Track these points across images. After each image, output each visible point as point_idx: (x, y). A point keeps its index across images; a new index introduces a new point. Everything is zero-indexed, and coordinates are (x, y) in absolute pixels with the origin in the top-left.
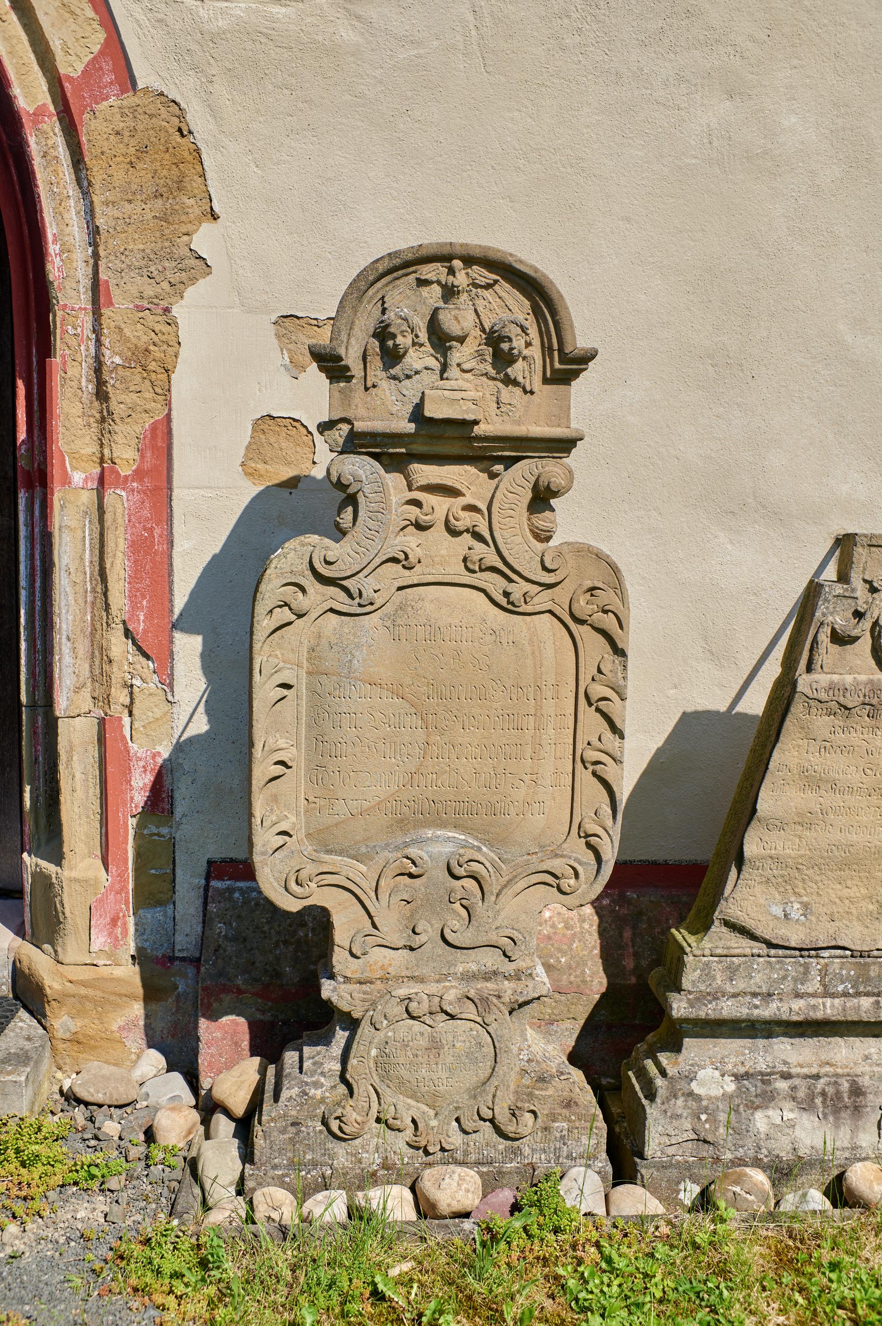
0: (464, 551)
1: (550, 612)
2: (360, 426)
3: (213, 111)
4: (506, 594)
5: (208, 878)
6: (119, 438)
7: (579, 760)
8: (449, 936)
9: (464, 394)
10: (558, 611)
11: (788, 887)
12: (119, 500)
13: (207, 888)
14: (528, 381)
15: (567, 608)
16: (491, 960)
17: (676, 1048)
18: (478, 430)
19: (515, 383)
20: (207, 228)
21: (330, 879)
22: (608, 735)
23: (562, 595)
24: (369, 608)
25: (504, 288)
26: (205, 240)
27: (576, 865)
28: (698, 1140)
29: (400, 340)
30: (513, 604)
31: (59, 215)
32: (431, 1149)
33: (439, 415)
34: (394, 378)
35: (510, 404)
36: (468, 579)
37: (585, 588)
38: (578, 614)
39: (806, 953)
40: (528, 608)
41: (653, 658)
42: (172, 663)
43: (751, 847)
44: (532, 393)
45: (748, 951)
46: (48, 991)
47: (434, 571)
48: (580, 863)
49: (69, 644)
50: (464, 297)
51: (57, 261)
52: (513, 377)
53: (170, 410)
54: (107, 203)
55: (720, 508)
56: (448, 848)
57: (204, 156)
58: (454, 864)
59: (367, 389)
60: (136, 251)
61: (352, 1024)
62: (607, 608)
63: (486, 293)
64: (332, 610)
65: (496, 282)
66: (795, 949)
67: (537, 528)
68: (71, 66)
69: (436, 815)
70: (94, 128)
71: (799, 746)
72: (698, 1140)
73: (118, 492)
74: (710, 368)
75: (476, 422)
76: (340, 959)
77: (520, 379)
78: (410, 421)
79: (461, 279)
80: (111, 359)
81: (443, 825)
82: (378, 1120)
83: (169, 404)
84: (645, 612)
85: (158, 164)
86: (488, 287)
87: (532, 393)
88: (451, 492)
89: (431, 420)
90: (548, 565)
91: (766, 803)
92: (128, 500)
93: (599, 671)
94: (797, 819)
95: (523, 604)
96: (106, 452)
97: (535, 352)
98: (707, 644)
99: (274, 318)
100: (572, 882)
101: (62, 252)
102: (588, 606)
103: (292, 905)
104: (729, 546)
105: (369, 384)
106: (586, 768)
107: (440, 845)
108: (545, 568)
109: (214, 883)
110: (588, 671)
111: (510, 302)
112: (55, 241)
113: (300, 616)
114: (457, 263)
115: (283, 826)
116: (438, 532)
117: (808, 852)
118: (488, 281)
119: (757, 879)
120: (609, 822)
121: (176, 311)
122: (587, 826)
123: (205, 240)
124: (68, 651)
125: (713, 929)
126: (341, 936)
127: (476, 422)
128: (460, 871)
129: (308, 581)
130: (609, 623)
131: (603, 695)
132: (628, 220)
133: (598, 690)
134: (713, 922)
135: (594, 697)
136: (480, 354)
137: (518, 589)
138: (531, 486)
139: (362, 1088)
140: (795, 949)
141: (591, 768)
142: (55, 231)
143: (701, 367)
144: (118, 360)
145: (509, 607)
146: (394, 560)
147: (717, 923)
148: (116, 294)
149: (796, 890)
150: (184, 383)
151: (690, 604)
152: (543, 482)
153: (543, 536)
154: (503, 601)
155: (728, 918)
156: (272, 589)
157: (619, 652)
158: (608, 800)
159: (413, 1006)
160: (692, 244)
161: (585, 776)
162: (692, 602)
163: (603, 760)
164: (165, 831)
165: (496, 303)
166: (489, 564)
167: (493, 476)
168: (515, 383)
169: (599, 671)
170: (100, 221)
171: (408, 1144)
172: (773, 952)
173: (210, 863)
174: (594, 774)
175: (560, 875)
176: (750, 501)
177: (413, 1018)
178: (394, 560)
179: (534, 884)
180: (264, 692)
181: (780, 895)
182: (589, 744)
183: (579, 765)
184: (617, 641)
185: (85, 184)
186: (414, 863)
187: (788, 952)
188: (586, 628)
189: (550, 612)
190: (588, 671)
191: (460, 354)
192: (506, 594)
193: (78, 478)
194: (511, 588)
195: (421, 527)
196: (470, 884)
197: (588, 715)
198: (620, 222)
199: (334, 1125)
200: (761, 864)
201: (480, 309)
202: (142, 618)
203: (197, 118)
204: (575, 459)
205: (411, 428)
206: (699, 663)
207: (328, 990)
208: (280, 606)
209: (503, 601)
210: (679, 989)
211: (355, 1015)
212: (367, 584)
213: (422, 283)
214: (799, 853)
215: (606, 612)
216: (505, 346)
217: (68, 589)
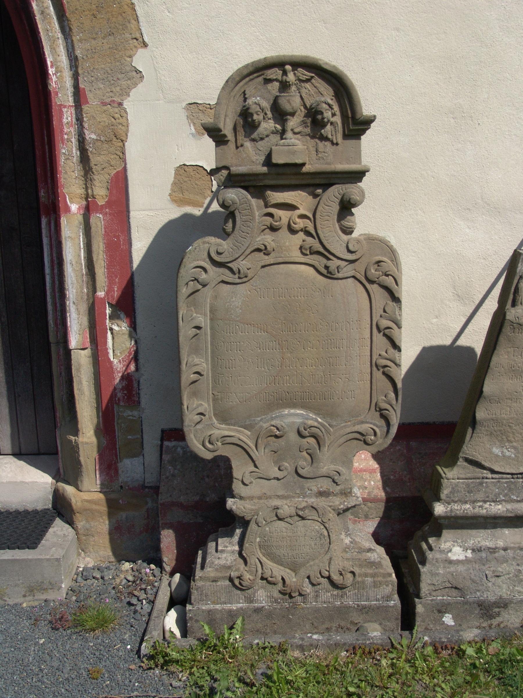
0: (300, 243)
1: (354, 277)
2: (235, 170)
4: (327, 267)
5: (162, 440)
6: (96, 183)
7: (375, 365)
8: (300, 471)
9: (296, 148)
10: (358, 276)
11: (504, 437)
12: (98, 221)
13: (161, 446)
14: (334, 137)
15: (363, 274)
16: (325, 485)
17: (438, 534)
18: (306, 169)
19: (326, 139)
20: (141, 52)
21: (229, 440)
22: (391, 350)
23: (360, 267)
24: (245, 280)
25: (318, 82)
26: (140, 60)
27: (375, 428)
28: (452, 587)
29: (255, 117)
30: (330, 273)
31: (53, 49)
32: (293, 595)
33: (281, 161)
34: (254, 140)
35: (324, 152)
36: (303, 259)
37: (374, 262)
38: (370, 277)
39: (516, 476)
40: (340, 275)
41: (422, 301)
42: (134, 315)
43: (480, 414)
44: (337, 144)
45: (480, 475)
46: (74, 507)
47: (283, 256)
48: (377, 426)
49: (74, 306)
50: (293, 88)
51: (54, 78)
52: (325, 135)
53: (126, 164)
54: (80, 41)
55: (461, 206)
56: (299, 420)
57: (137, 8)
58: (302, 429)
59: (237, 147)
60: (100, 69)
61: (245, 523)
62: (388, 273)
63: (308, 85)
64: (223, 282)
65: (312, 77)
66: (508, 474)
67: (344, 226)
71: (508, 352)
72: (452, 587)
73: (98, 215)
74: (452, 121)
75: (303, 164)
76: (237, 487)
77: (330, 136)
78: (263, 165)
79: (291, 77)
80: (90, 136)
81: (294, 406)
82: (262, 578)
83: (125, 161)
84: (417, 273)
85: (110, 14)
86: (308, 81)
87: (337, 144)
88: (291, 207)
89: (277, 165)
90: (351, 248)
91: (489, 387)
92: (104, 220)
93: (385, 311)
94: (508, 396)
95: (337, 273)
96: (90, 191)
97: (338, 119)
98: (455, 290)
99: (184, 104)
100: (373, 438)
101: (57, 72)
102: (376, 273)
103: (209, 456)
104: (467, 230)
105: (239, 144)
106: (379, 370)
107: (293, 417)
108: (349, 251)
109: (166, 443)
110: (378, 311)
111: (322, 89)
112: (52, 66)
113: (204, 286)
114: (288, 67)
115: (200, 410)
116: (284, 233)
117: (515, 416)
118: (307, 77)
119: (485, 433)
120: (394, 402)
121: (126, 104)
122: (380, 404)
123: (140, 60)
124: (74, 310)
125: (459, 463)
126: (237, 473)
127: (303, 164)
128: (306, 433)
129: (207, 265)
130: (389, 281)
131: (386, 326)
132: (398, 29)
133: (385, 323)
134: (458, 459)
135: (382, 327)
136: (304, 122)
137: (334, 263)
138: (338, 201)
139: (253, 560)
140: (508, 474)
141: (382, 370)
142: (51, 60)
143: (446, 119)
144: (93, 136)
145: (329, 274)
146: (258, 250)
147: (461, 460)
148: (90, 96)
149: (509, 439)
150: (133, 148)
151: (444, 267)
152: (346, 198)
153: (348, 231)
154: (325, 272)
155: (467, 456)
156: (188, 270)
157: (396, 300)
158: (392, 389)
159: (280, 511)
160: (438, 42)
161: (378, 375)
162: (445, 265)
163: (389, 365)
164: (136, 413)
165: (313, 91)
166: (316, 250)
167: (315, 196)
168: (326, 139)
169: (385, 311)
170: (78, 53)
171: (280, 592)
172: (495, 476)
173: (163, 431)
174: (384, 373)
175: (365, 434)
176: (480, 201)
177: (280, 519)
178: (258, 250)
179: (350, 440)
181: (499, 442)
182: (380, 355)
183: (374, 368)
184: (395, 292)
185: (68, 30)
186: (278, 429)
187: (505, 476)
188: (375, 286)
189: (354, 277)
190: (378, 311)
191: (293, 123)
192: (327, 267)
193: (74, 208)
194: (329, 263)
195: (273, 229)
196: (312, 440)
197: (379, 338)
198: (393, 32)
199: (237, 582)
200: (487, 424)
201: (304, 95)
202: (116, 289)
204: (365, 183)
205: (265, 169)
206: (451, 302)
207: (230, 503)
208: (192, 281)
209: (325, 272)
210: (439, 499)
211: (247, 518)
212: (243, 264)
213: (268, 81)
214: (510, 416)
215: (387, 275)
216: (319, 117)
217: (72, 274)
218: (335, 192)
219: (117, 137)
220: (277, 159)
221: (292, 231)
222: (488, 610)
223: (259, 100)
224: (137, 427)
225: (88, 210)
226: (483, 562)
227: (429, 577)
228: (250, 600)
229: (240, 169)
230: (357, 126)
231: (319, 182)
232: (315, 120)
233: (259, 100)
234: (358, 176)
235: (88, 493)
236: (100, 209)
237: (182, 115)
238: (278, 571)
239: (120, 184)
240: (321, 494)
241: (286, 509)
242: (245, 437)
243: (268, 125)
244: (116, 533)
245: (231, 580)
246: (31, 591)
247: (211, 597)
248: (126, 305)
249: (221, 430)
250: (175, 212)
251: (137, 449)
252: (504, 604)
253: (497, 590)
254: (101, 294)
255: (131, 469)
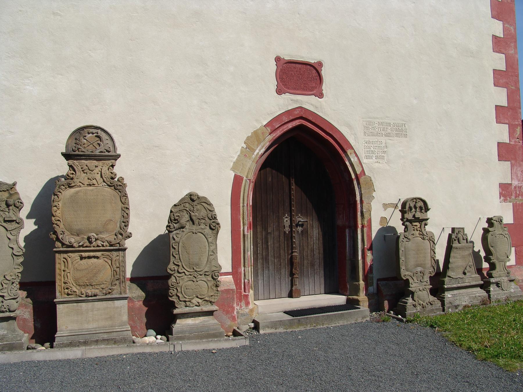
3: (374, 178)
7: (431, 257)
9: (418, 215)
12: (365, 229)
16: (425, 283)
26: (374, 194)
43: (450, 266)
61: (413, 293)
68: (358, 173)
69: (418, 266)
70: (362, 180)
76: (411, 285)
80: (364, 210)
88: (416, 226)
91: (451, 260)
107: (419, 269)
123: (374, 194)
126: (410, 282)
137: (425, 237)
139: (416, 300)
145: (424, 239)
153: (425, 230)
180: (401, 252)
191: (418, 209)
203: (373, 179)
212: (410, 237)
218: (424, 223)
219: (370, 211)
220: (416, 216)
221: (417, 230)
222: (456, 307)
223: (412, 205)
224: (372, 279)
225: (363, 227)
226: (454, 297)
227: (446, 301)
228: (417, 310)
229: (409, 218)
230: (427, 209)
231: (420, 221)
232: (421, 208)
233: (412, 205)
234: (427, 219)
235: (362, 296)
236: (366, 227)
237: (382, 206)
238: (422, 302)
239: (370, 221)
240: (425, 285)
241: (421, 289)
242: (411, 274)
243: (413, 210)
244: (370, 306)
245: (413, 305)
246: (363, 318)
247: (410, 311)
248: (371, 249)
249: (407, 273)
250: (381, 227)
251: (372, 285)
252: (459, 306)
253: (457, 303)
254: (366, 246)
255: (371, 289)
